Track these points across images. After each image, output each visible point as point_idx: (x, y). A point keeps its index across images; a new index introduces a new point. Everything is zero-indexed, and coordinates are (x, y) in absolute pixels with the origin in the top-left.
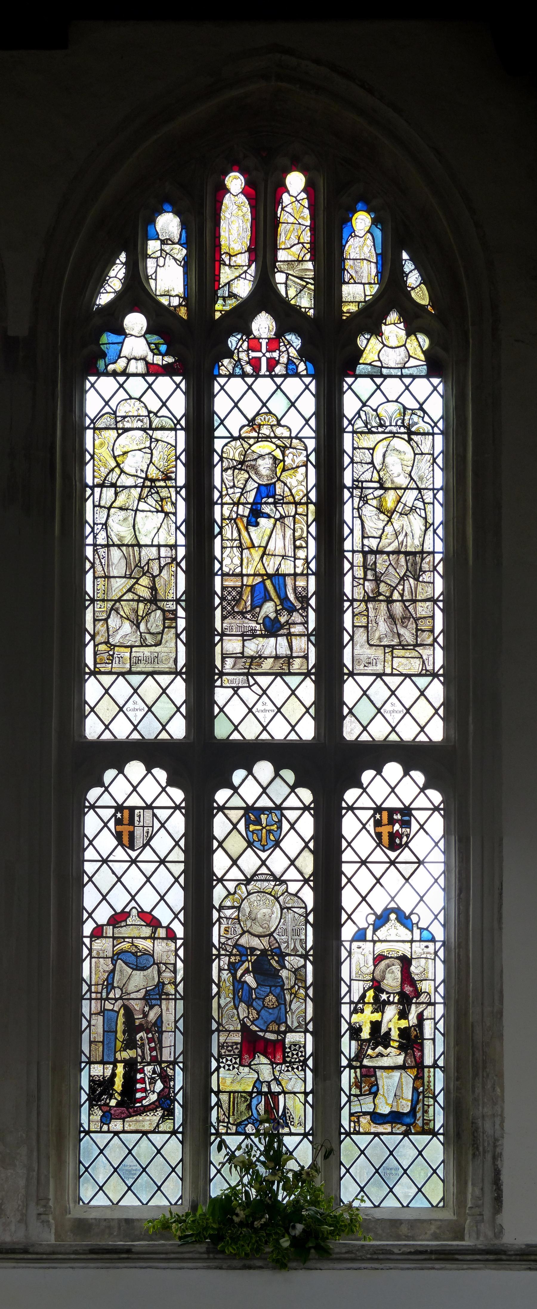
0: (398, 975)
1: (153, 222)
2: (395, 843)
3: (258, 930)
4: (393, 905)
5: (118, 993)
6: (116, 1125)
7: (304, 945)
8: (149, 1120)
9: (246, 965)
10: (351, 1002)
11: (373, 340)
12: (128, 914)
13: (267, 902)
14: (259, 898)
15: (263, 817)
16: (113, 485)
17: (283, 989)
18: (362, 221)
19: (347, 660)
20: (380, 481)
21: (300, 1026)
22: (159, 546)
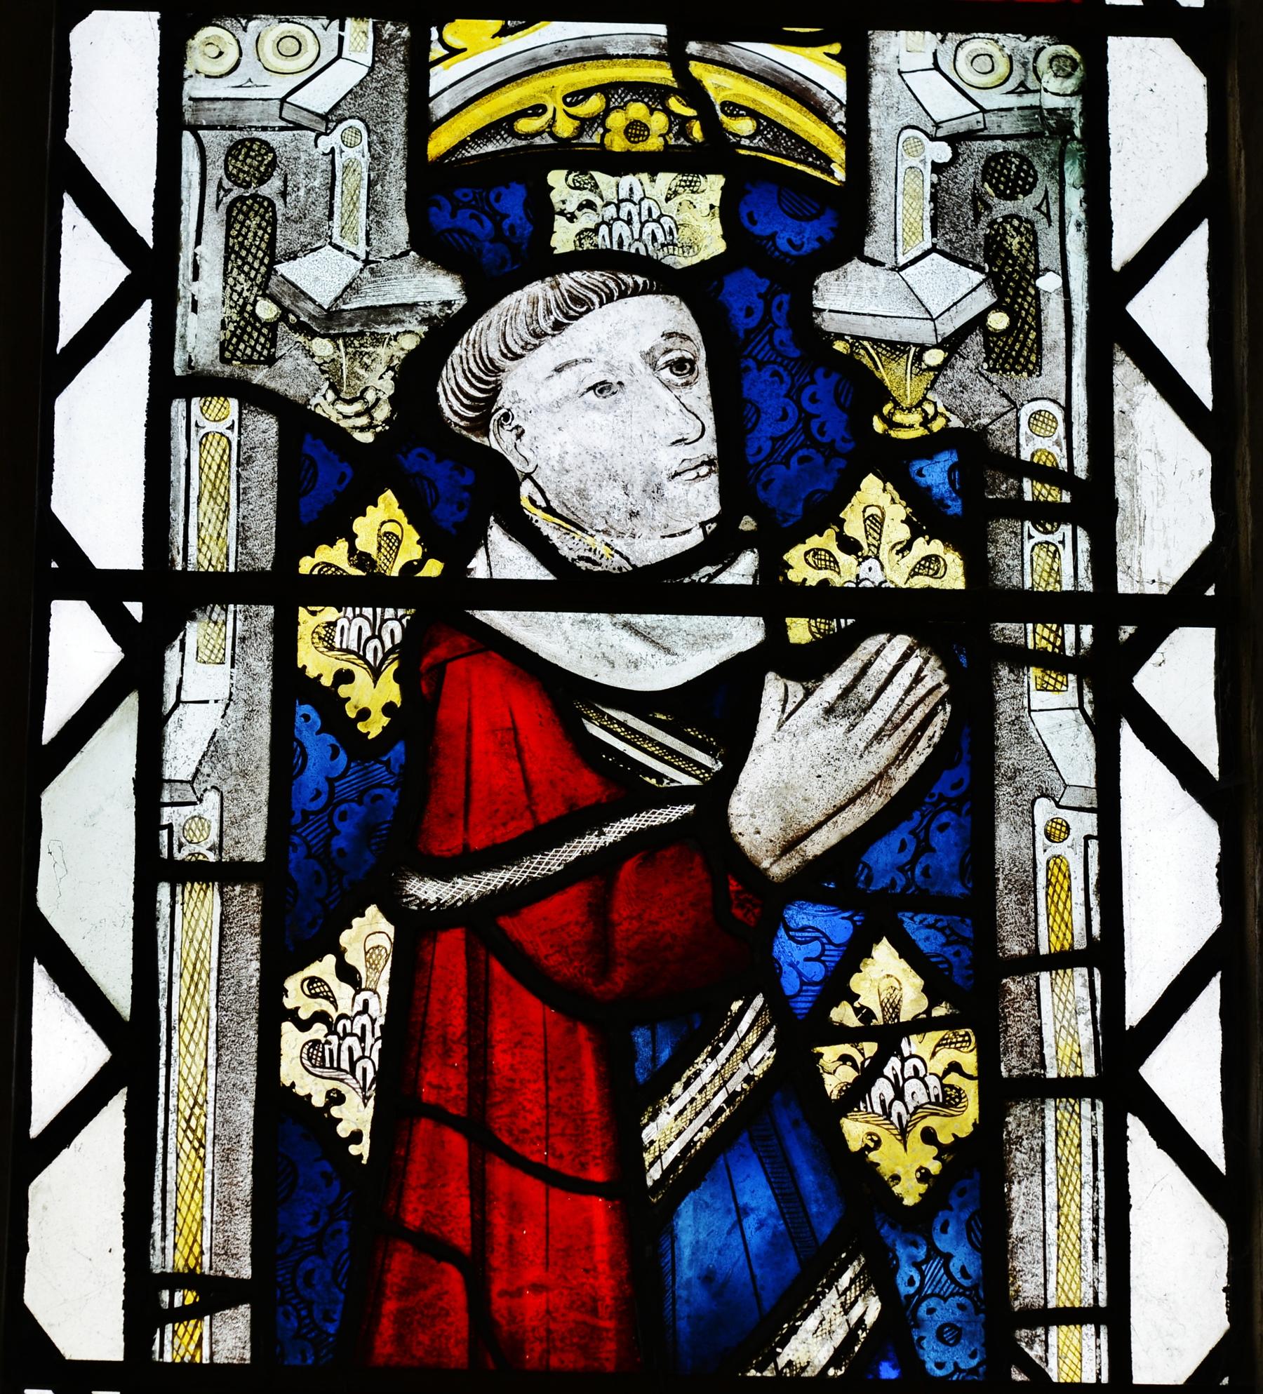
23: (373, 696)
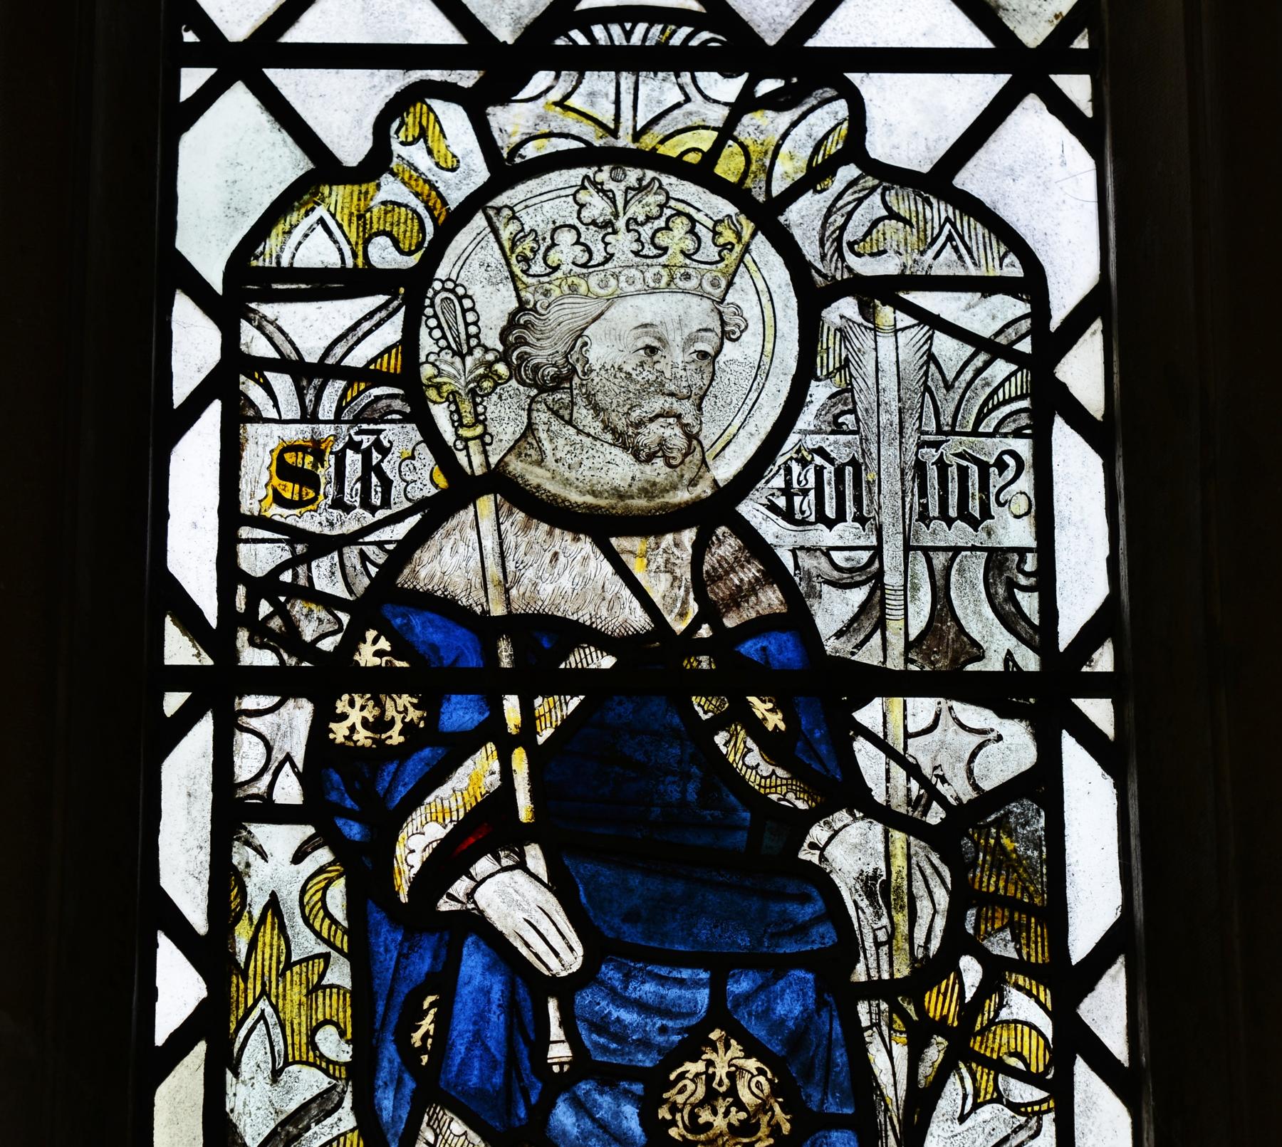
3: (592, 467)
7: (1029, 603)
9: (477, 774)
13: (677, 239)
14: (597, 207)
17: (838, 990)
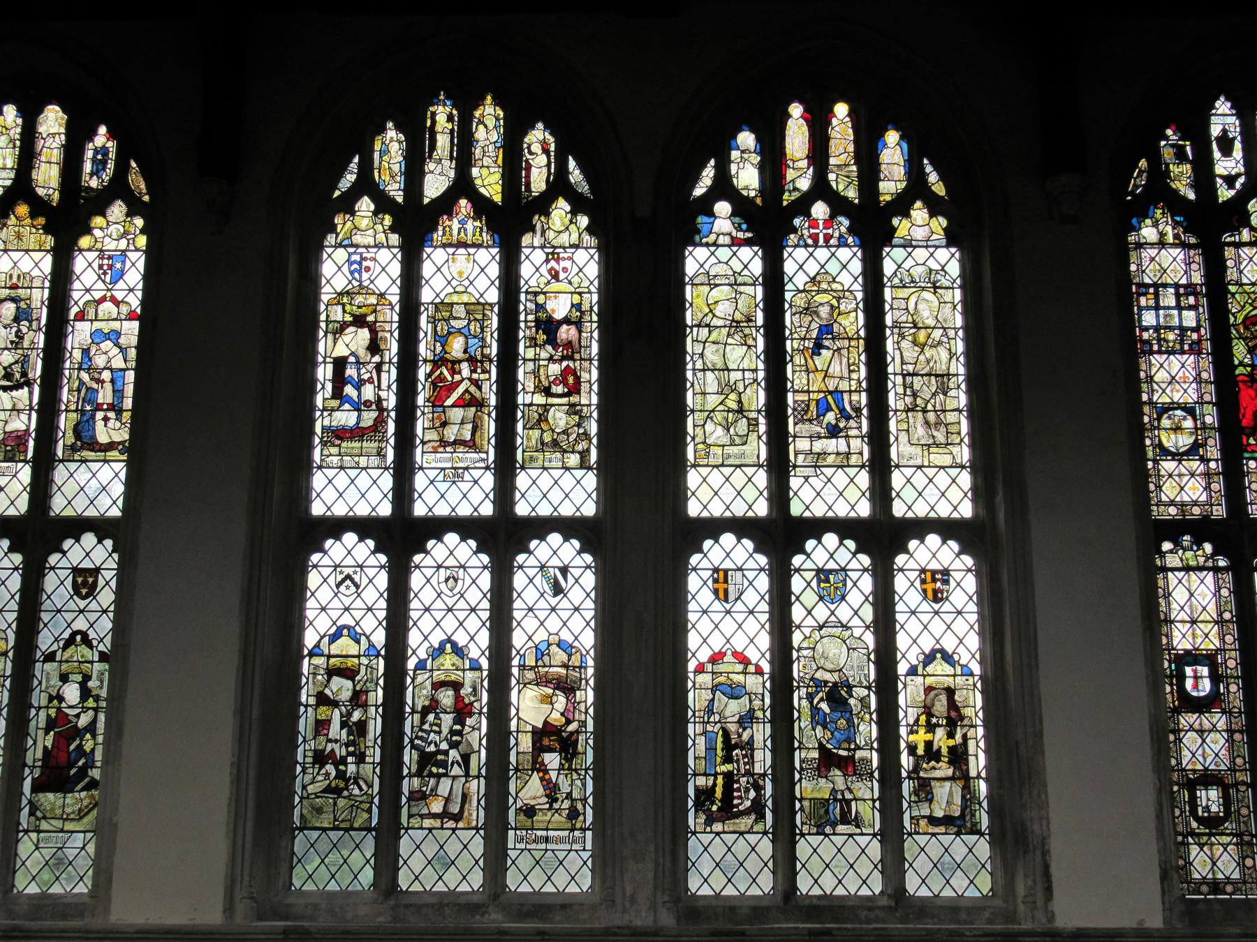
0: (945, 702)
1: (735, 138)
2: (937, 597)
3: (829, 666)
4: (938, 646)
5: (717, 718)
6: (718, 827)
8: (745, 822)
10: (908, 725)
11: (904, 221)
12: (725, 654)
15: (831, 577)
16: (708, 326)
18: (892, 137)
19: (894, 455)
20: (914, 322)
21: (866, 744)
22: (743, 370)
23: (53, 715)
